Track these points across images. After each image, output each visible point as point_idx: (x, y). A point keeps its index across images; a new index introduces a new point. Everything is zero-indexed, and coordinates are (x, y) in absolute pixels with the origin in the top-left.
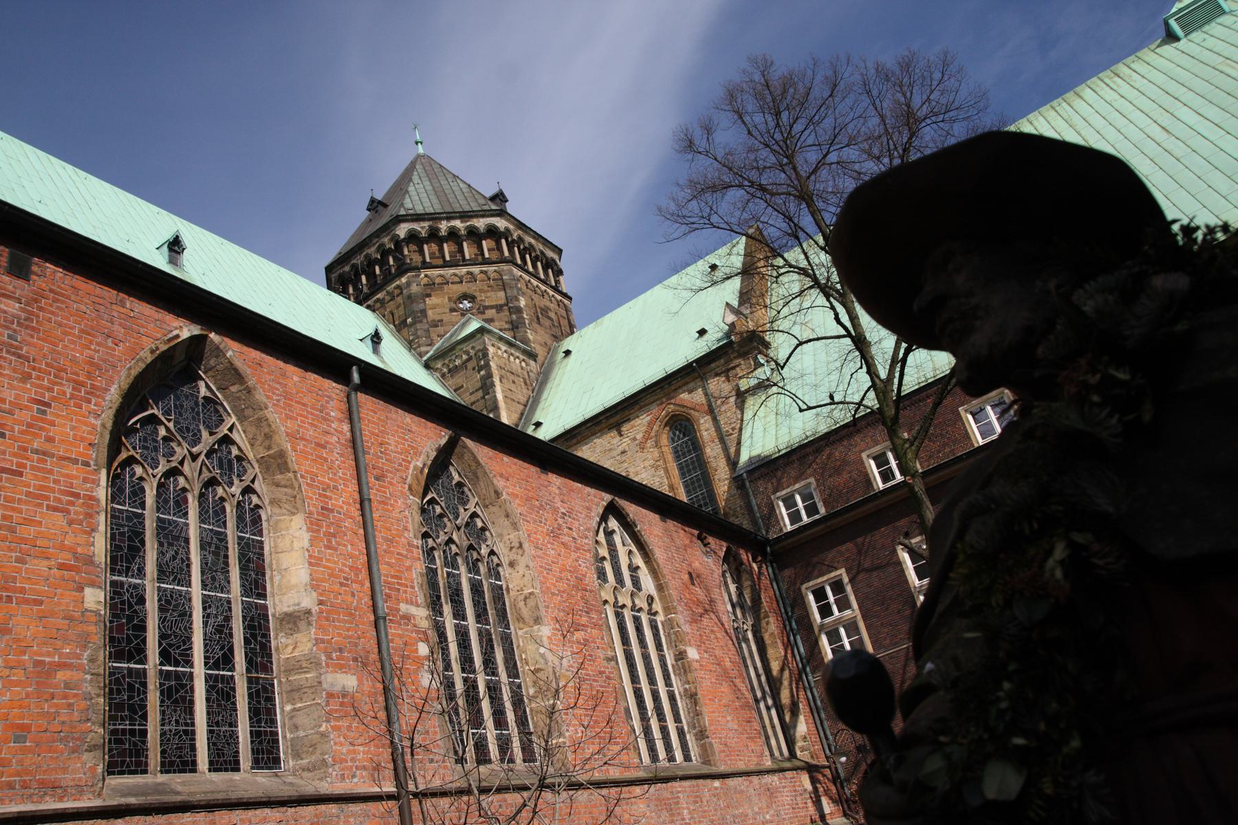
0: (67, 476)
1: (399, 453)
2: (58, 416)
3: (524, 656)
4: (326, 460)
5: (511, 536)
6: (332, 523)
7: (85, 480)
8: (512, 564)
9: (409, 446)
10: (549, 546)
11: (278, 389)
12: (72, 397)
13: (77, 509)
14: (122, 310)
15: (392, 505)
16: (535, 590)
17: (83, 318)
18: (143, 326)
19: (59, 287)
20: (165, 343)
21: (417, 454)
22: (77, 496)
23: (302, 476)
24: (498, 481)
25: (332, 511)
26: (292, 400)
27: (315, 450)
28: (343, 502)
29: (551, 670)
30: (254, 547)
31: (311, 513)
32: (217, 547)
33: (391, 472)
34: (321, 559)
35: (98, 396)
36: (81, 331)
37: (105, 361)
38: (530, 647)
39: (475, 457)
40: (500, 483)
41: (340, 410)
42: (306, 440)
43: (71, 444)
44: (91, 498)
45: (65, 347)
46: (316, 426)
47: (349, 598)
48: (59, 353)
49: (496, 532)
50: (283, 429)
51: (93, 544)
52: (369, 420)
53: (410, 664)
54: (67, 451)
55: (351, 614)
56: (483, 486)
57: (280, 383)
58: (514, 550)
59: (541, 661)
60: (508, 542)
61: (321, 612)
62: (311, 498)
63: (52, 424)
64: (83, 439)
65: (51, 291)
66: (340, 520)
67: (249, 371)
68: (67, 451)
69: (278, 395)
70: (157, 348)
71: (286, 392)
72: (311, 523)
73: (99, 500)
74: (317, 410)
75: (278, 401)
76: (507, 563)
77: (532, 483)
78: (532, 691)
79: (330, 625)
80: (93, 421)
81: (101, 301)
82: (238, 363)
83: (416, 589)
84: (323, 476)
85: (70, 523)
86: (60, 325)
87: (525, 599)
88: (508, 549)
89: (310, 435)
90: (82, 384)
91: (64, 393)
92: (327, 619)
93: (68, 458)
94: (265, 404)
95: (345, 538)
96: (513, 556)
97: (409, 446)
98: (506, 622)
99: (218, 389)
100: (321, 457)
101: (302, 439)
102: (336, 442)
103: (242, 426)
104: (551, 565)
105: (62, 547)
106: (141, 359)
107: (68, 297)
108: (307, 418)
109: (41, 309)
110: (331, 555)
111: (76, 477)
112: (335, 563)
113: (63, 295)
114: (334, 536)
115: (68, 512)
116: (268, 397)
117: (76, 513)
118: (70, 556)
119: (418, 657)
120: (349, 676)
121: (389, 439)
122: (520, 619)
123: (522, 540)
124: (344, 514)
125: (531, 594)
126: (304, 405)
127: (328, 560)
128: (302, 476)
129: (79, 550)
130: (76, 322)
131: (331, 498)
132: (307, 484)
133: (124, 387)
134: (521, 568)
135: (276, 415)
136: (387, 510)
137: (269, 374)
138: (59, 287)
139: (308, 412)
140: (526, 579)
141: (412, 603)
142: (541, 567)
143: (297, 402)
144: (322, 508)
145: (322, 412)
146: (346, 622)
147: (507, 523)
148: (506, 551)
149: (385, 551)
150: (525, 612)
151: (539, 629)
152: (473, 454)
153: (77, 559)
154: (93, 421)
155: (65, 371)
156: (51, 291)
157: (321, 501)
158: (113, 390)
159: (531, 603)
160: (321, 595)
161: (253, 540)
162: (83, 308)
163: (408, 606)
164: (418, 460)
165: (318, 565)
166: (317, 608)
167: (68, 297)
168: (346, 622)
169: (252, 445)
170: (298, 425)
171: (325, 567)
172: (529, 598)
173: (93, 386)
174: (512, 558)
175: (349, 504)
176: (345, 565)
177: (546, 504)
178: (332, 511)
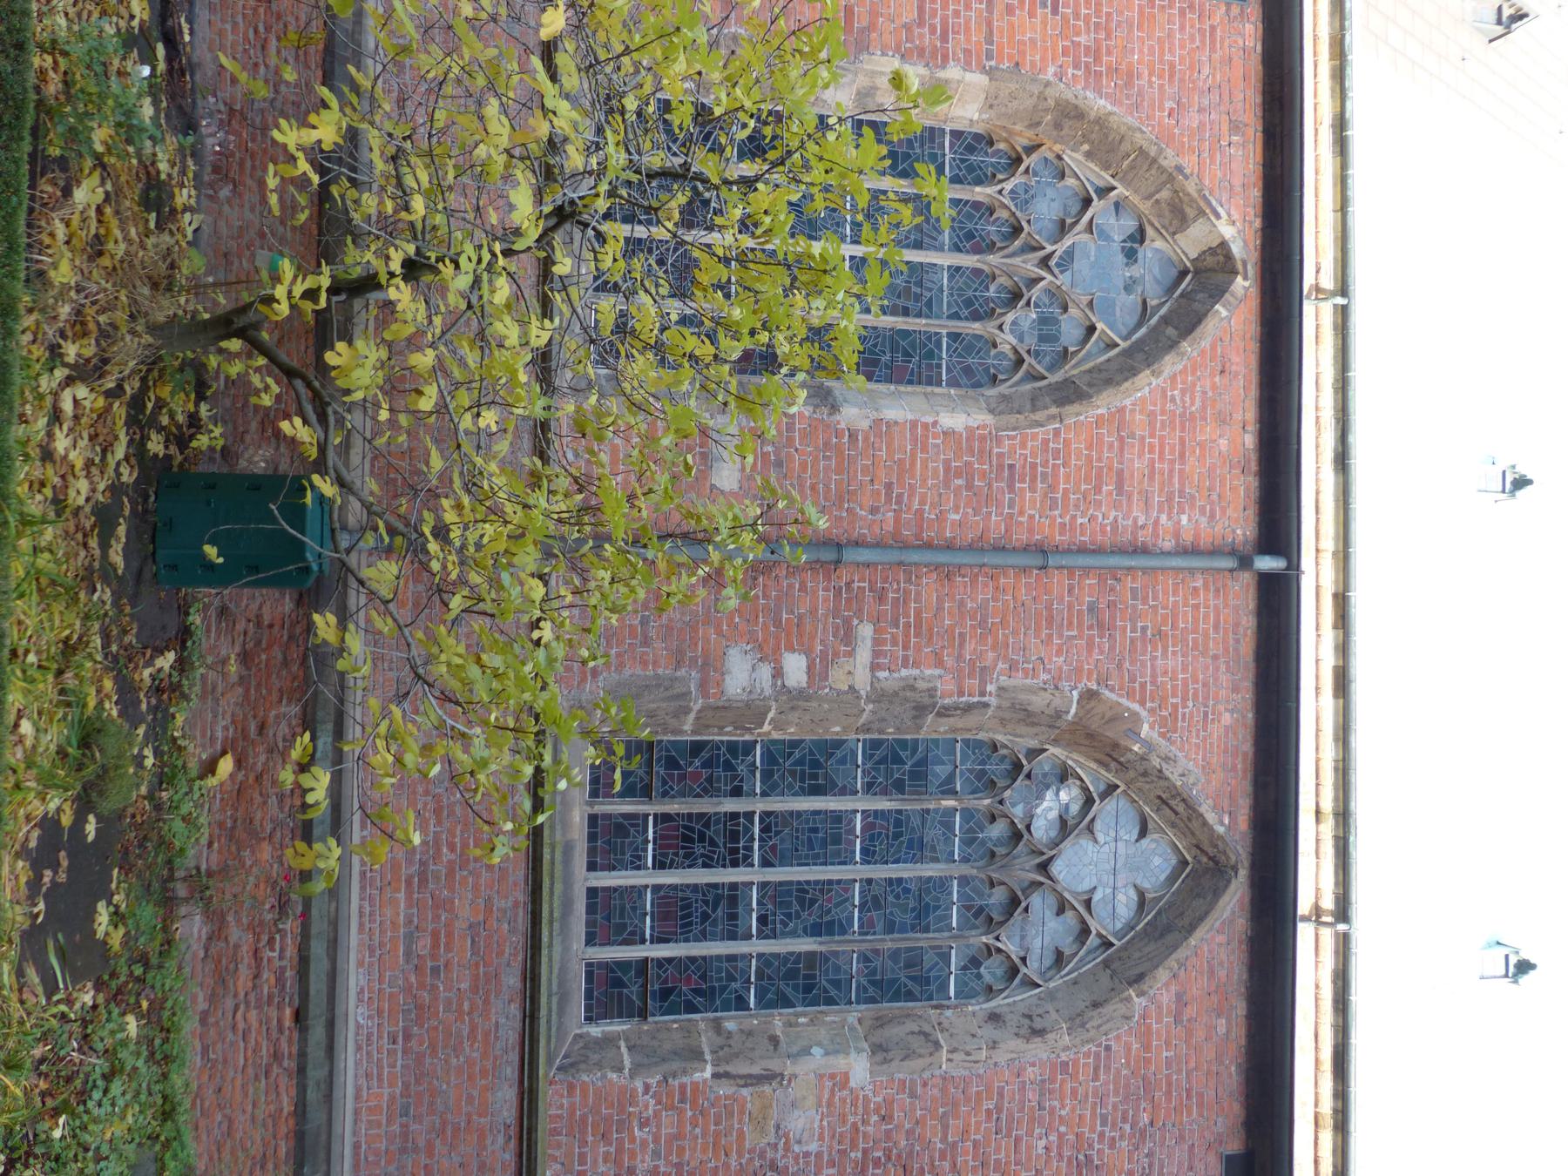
0: (967, 30)
1: (1154, 676)
2: (1044, 23)
3: (802, 1020)
4: (1098, 490)
5: (1054, 1015)
6: (990, 486)
7: (967, 52)
8: (994, 1017)
9: (1175, 706)
10: (1053, 1138)
11: (1192, 404)
12: (1077, 45)
13: (926, 38)
14: (1225, 127)
15: (1050, 636)
16: (944, 1054)
17: (1192, 68)
18: (1212, 157)
19: (1222, 40)
20: (1200, 191)
21: (1168, 726)
22: (944, 39)
23: (1057, 432)
24: (1167, 985)
25: (1011, 488)
26: (1183, 430)
27: (1110, 469)
28: (1031, 517)
29: (774, 1065)
30: (930, 367)
31: (999, 441)
32: (918, 297)
33: (1112, 648)
34: (924, 450)
35: (1086, 81)
36: (1172, 65)
37: (1140, 94)
38: (823, 1032)
39: (1201, 919)
40: (1162, 986)
41: (1197, 536)
42: (1122, 450)
43: (1011, 37)
44: (945, 58)
45: (1141, 40)
46: (1151, 478)
47: (868, 502)
48: (1130, 31)
49: (1057, 989)
50: (1128, 402)
51: (883, 54)
52: (1196, 607)
53: (764, 624)
54: (1001, 32)
55: (841, 499)
56: (1146, 950)
57: (1204, 408)
58: (1027, 1022)
59: (795, 1049)
60: (1040, 1011)
61: (839, 434)
62: (1023, 445)
63: (1032, 15)
64: (1022, 53)
65: (1213, 28)
66: (999, 505)
67: (1206, 343)
68: (1001, 32)
69: (1183, 402)
70: (1186, 178)
71: (1193, 418)
72: (982, 439)
73: (944, 67)
74: (1182, 484)
75: (1173, 400)
76: (998, 1011)
77: (1189, 1114)
78: (730, 1025)
79: (817, 448)
80: (1051, 70)
81: (1226, 97)
82: (1210, 328)
83: (904, 673)
84: (1068, 476)
85: (908, 27)
86: (1170, 35)
87: (926, 1035)
88: (1026, 1012)
89: (1132, 460)
90: (1097, 59)
91: (1078, 34)
92: (826, 444)
93: (991, 32)
94: (1160, 373)
95: (970, 511)
96: (1013, 1020)
97: (1175, 706)
98: (871, 991)
99: (1162, 317)
100: (1099, 476)
101: (1121, 439)
102: (1135, 520)
103: (1118, 355)
104: (1008, 1135)
105: (874, 14)
106: (1161, 151)
107: (1213, 49)
108: (1161, 459)
109: (1182, 13)
110: (936, 470)
111: (968, 40)
112: (924, 481)
113: (1213, 41)
114: (969, 486)
115: (921, 24)
116: (1173, 378)
117: (921, 36)
118: (865, 24)
119: (777, 649)
120: (737, 475)
121: (1174, 653)
122: (880, 1022)
123: (1050, 1036)
124: (1011, 516)
125: (937, 1045)
126: (1182, 455)
127: (925, 466)
128: (1057, 432)
129: (874, 35)
130: (1182, 58)
131: (1033, 489)
132: (1046, 442)
133: (1111, 118)
134: (989, 1031)
135: (1147, 389)
136: (1038, 629)
137: (1214, 387)
138: (1222, 40)
139: (1172, 462)
140: (968, 1038)
141: (876, 654)
142: (1001, 1095)
143: (1182, 441)
144: (1011, 467)
145: (1182, 493)
146: (827, 487)
147: (1082, 1005)
148: (1021, 1008)
149: (962, 603)
150: (895, 1032)
151: (863, 1050)
152: (1207, 913)
153: (862, 31)
154: (1051, 70)
155: (1108, 37)
156: (1213, 28)
157: (1024, 467)
158: (1102, 102)
159: (917, 1043)
160: (866, 439)
161: (939, 366)
162: (1206, 71)
163: (869, 643)
164: (1152, 727)
165: (914, 440)
166: (843, 425)
167: (1213, 49)
168: (827, 487)
169: (1090, 371)
170: (1143, 438)
171: (913, 454)
172: (928, 1041)
173: (1099, 74)
174: (1008, 1017)
175: (1031, 530)
176: (923, 502)
177: (1150, 1155)
178: (1011, 488)
